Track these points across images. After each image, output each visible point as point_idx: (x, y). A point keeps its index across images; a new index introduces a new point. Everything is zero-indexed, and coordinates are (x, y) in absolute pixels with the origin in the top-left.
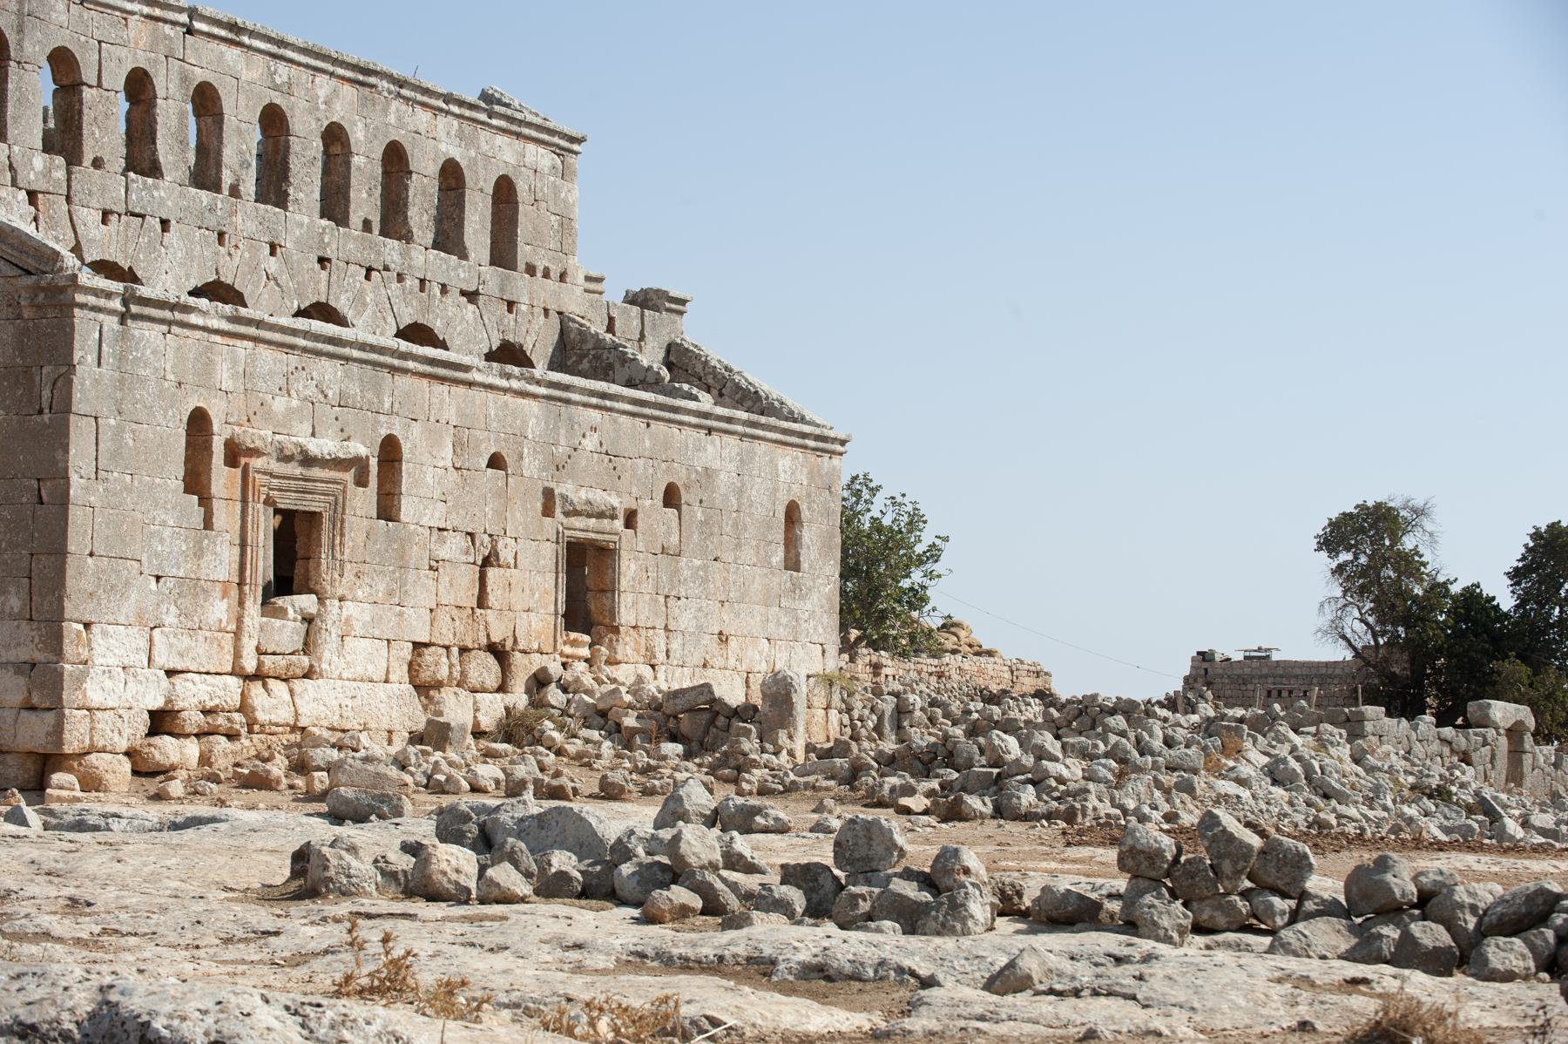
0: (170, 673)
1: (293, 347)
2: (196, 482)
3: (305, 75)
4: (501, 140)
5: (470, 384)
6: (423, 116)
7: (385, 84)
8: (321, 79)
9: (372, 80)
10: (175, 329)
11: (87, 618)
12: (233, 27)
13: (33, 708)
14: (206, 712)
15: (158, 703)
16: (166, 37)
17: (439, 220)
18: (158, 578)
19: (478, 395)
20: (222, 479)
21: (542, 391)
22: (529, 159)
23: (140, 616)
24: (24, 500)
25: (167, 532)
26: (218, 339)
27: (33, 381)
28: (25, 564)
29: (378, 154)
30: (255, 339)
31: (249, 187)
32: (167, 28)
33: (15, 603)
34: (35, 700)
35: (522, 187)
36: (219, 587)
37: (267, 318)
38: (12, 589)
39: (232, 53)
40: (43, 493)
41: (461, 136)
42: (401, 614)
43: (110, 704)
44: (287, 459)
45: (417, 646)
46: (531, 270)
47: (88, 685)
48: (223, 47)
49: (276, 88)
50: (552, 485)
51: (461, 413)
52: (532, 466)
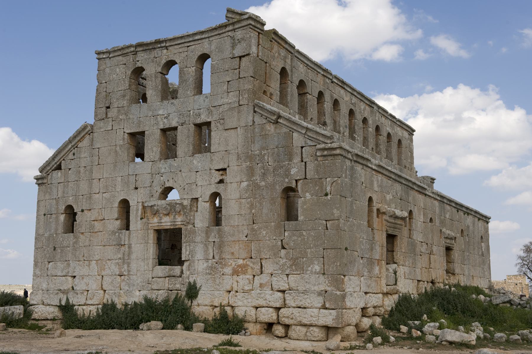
0: (366, 293)
1: (391, 178)
2: (370, 224)
3: (359, 101)
4: (399, 129)
5: (426, 195)
6: (383, 119)
7: (375, 107)
8: (362, 103)
9: (373, 105)
10: (365, 167)
11: (345, 273)
12: (343, 82)
13: (326, 309)
14: (375, 307)
15: (363, 305)
16: (327, 83)
17: (387, 150)
18: (362, 258)
19: (428, 199)
20: (376, 221)
21: (439, 198)
22: (404, 135)
23: (358, 272)
24: (320, 228)
25: (364, 241)
26: (374, 172)
27: (323, 184)
28: (321, 253)
29: (374, 128)
30: (382, 174)
31: (347, 134)
32: (327, 80)
33: (317, 268)
34: (327, 306)
35: (403, 142)
36: (377, 261)
37: (385, 166)
38: (316, 263)
39: (342, 91)
40: (328, 225)
41: (391, 126)
42: (415, 271)
43: (352, 306)
44: (391, 216)
45: (419, 281)
46: (405, 167)
47: (347, 300)
48: (340, 89)
49: (352, 104)
50: (441, 228)
51: (424, 205)
52: (437, 222)
